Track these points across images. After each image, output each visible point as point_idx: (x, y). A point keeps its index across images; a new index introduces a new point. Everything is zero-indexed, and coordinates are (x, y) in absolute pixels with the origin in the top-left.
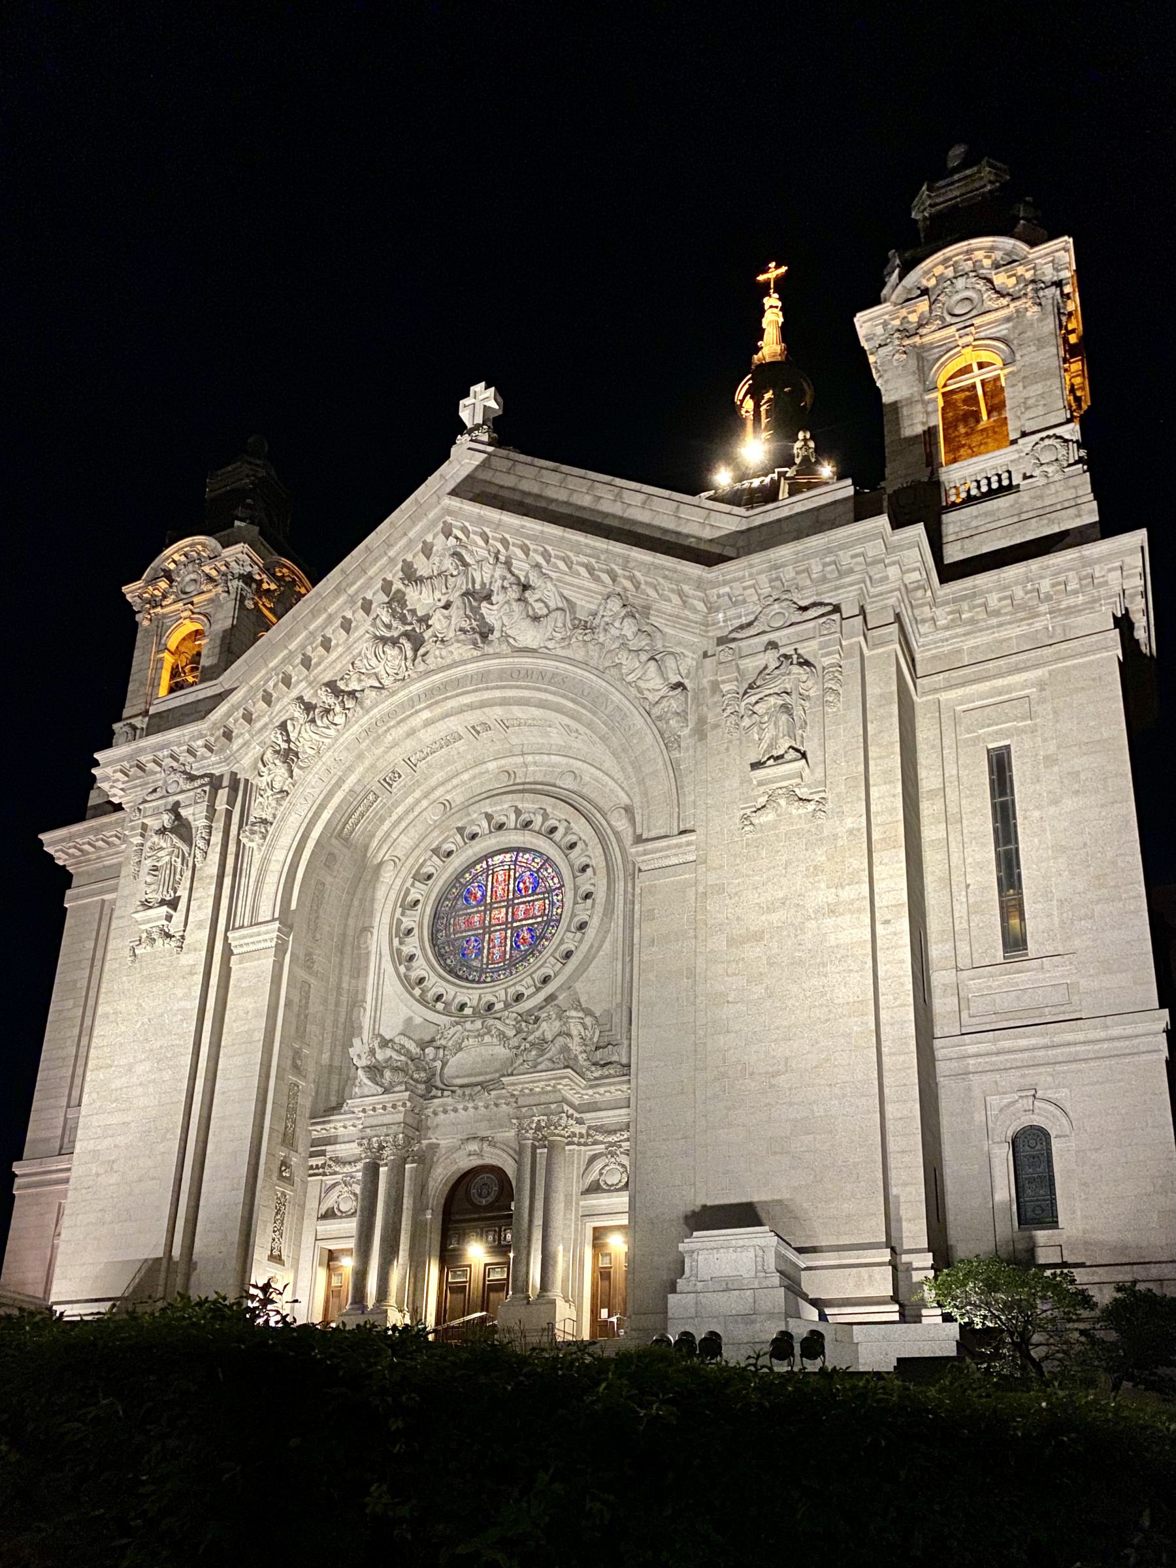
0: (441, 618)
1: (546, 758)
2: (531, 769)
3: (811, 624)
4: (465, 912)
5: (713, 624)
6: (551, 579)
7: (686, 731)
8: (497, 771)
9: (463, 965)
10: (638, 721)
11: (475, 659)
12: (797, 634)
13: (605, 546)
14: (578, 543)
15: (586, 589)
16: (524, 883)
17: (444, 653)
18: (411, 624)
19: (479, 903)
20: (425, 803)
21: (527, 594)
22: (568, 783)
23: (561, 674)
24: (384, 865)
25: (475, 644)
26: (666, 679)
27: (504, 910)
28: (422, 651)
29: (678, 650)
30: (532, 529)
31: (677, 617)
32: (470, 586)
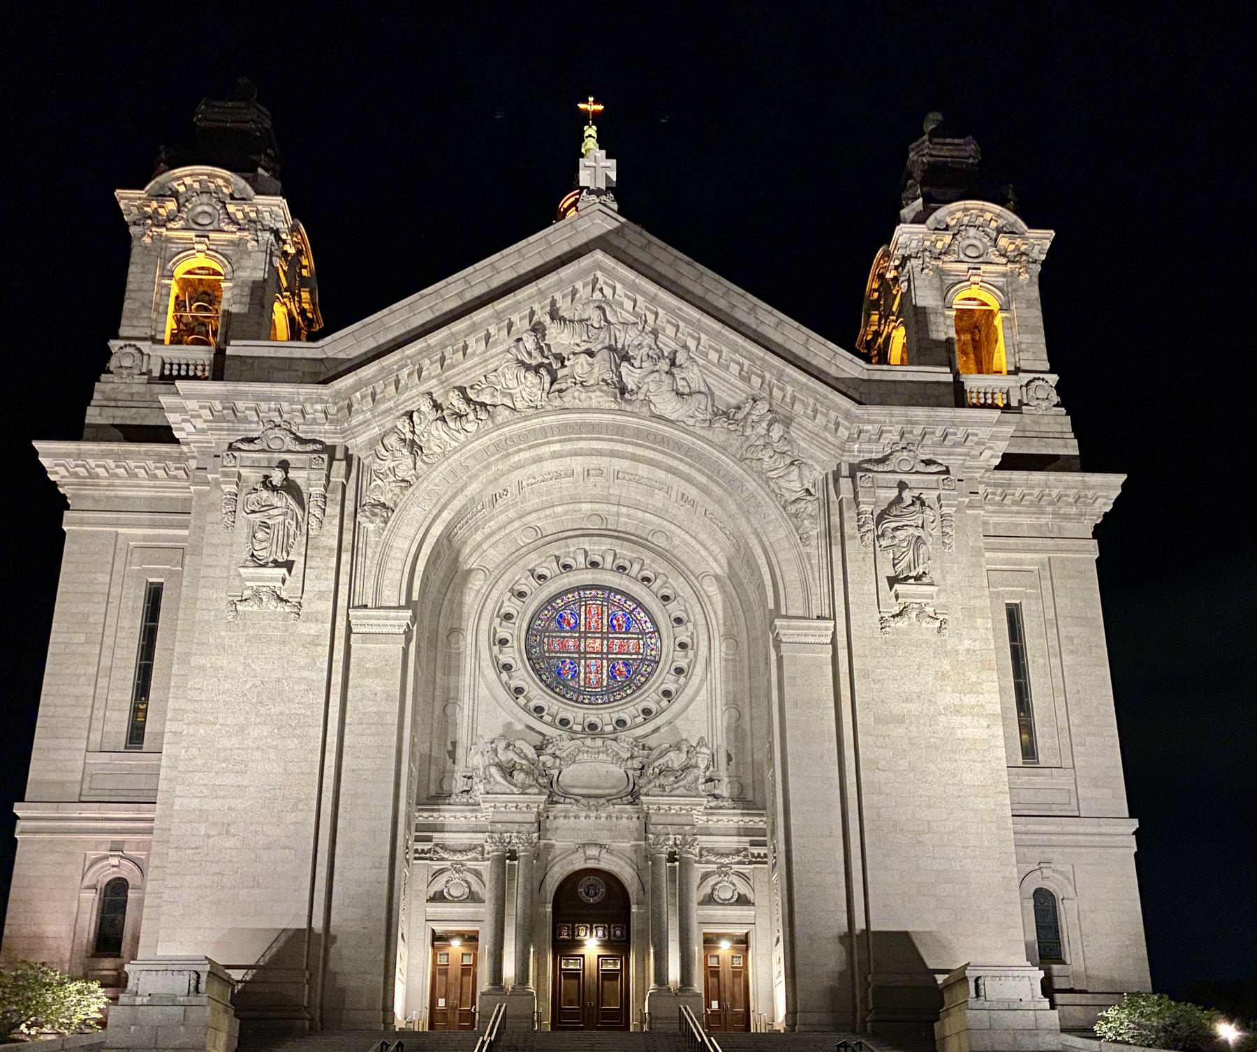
0: (585, 363)
1: (640, 514)
2: (622, 519)
3: (935, 477)
4: (558, 634)
5: (849, 451)
6: (698, 365)
7: (814, 533)
8: (589, 513)
9: (558, 683)
10: (773, 511)
11: (610, 411)
12: (924, 481)
13: (762, 355)
14: (736, 343)
15: (731, 384)
16: (618, 621)
17: (583, 396)
18: (547, 358)
19: (573, 629)
20: (517, 524)
21: (674, 370)
22: (660, 541)
23: (697, 451)
24: (473, 574)
25: (616, 398)
26: (803, 485)
27: (598, 641)
28: (556, 387)
29: (810, 462)
30: (689, 315)
31: (817, 435)
32: (613, 342)
